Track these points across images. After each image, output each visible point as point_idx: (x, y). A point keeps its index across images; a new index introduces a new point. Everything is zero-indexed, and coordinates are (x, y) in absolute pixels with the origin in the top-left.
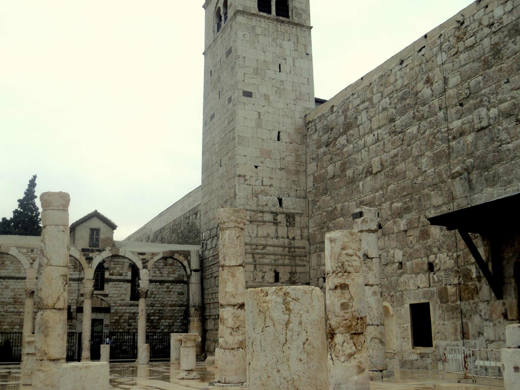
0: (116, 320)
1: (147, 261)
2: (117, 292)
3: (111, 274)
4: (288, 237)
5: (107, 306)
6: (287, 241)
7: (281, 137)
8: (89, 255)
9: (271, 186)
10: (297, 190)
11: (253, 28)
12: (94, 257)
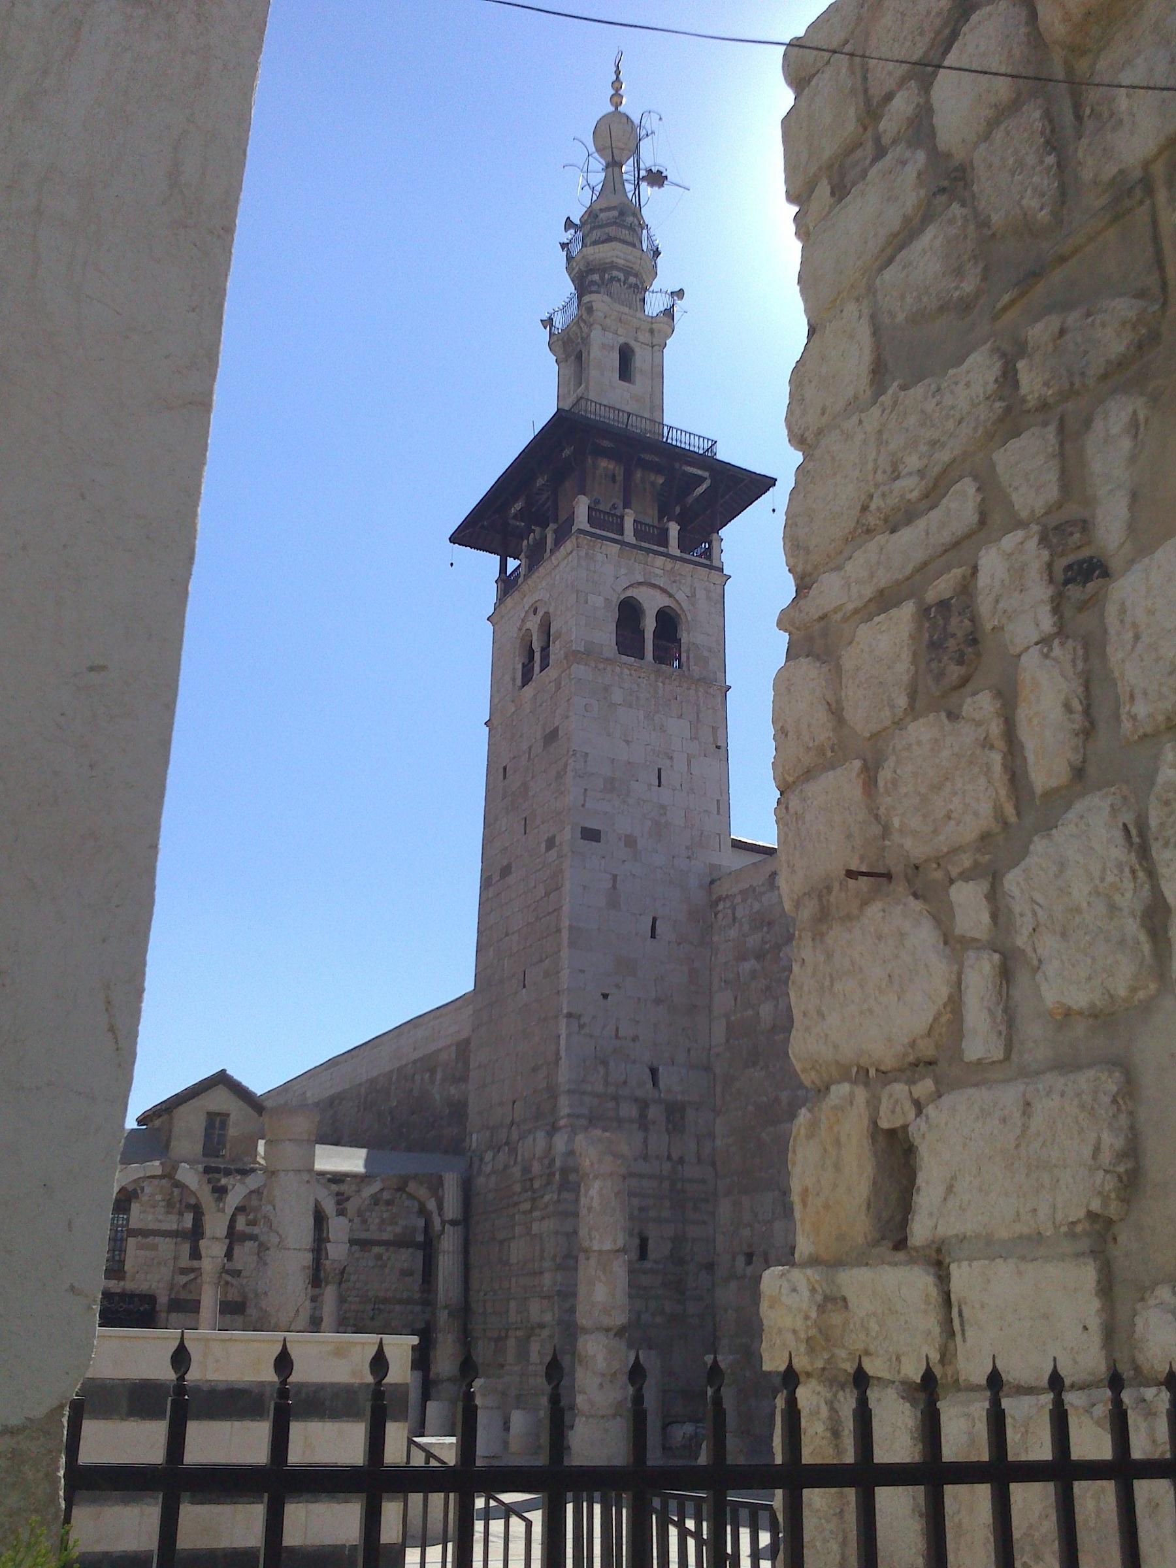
1: (348, 1199)
4: (669, 1158)
5: (239, 1299)
6: (667, 1166)
7: (658, 931)
8: (219, 1180)
9: (635, 1039)
10: (689, 1050)
11: (607, 689)
12: (230, 1187)
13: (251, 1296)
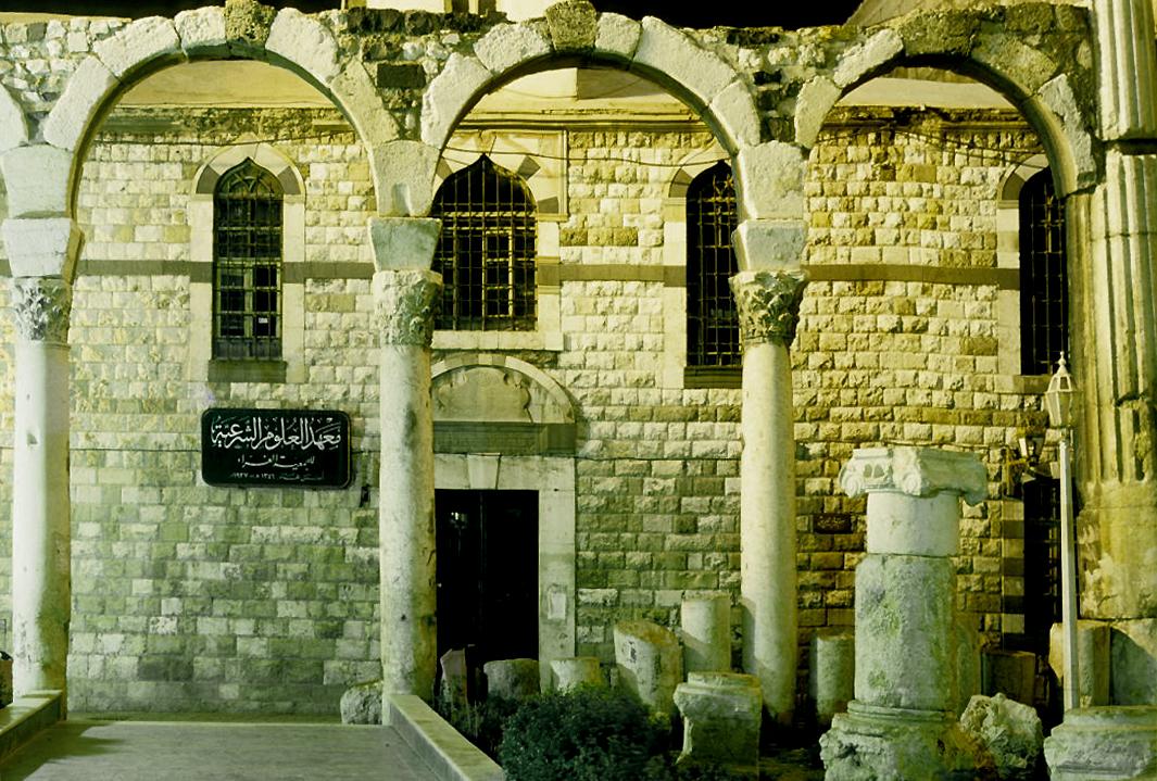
0: (610, 498)
2: (602, 340)
3: (569, 240)
12: (429, 66)
13: (590, 411)
